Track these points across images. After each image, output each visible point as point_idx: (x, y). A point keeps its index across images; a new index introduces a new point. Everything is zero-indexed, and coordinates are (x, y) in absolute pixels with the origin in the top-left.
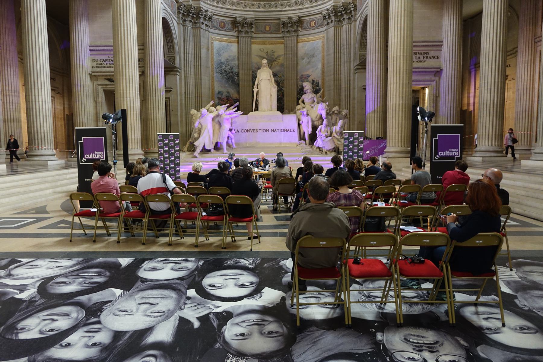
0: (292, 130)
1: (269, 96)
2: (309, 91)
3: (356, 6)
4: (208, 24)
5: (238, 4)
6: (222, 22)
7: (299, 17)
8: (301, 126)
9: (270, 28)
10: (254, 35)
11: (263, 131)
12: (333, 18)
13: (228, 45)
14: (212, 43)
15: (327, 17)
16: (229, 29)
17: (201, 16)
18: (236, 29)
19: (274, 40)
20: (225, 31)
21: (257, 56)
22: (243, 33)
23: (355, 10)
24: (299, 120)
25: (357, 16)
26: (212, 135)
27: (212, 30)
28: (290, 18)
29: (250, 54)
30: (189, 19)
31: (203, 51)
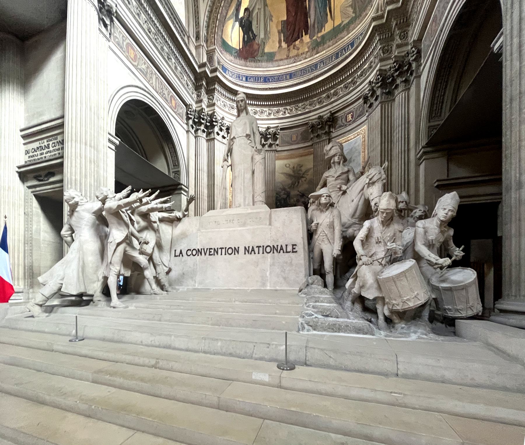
5: (262, 112)
7: (332, 114)
8: (316, 237)
11: (227, 250)
17: (215, 123)
24: (309, 222)
28: (320, 117)
30: (202, 127)
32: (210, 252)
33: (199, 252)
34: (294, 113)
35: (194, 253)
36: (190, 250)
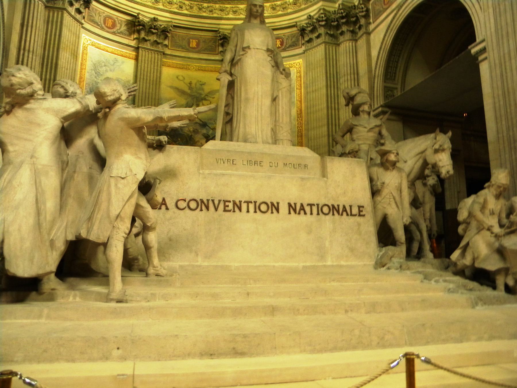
0: (355, 211)
1: (267, 102)
2: (366, 108)
3: (368, 11)
4: (82, 10)
6: (110, 18)
9: (198, 44)
10: (168, 52)
12: (322, 31)
13: (116, 60)
14: (85, 48)
15: (309, 29)
16: (121, 33)
18: (135, 37)
19: (204, 65)
20: (114, 33)
21: (171, 87)
22: (148, 43)
23: (367, 16)
25: (372, 27)
26: (51, 204)
27: (86, 25)
29: (158, 82)
31: (64, 57)
32: (225, 206)
33: (203, 205)
34: (195, 11)
35: (193, 205)
36: (185, 200)
